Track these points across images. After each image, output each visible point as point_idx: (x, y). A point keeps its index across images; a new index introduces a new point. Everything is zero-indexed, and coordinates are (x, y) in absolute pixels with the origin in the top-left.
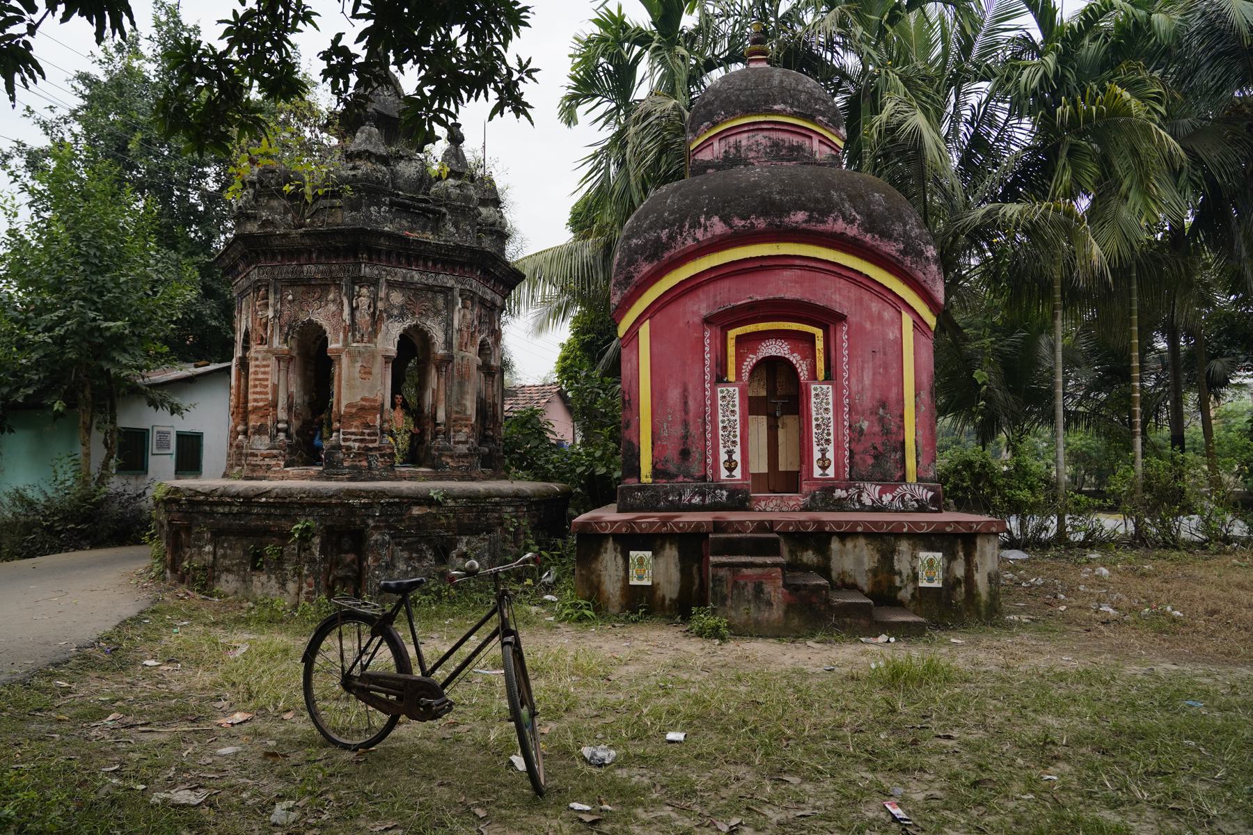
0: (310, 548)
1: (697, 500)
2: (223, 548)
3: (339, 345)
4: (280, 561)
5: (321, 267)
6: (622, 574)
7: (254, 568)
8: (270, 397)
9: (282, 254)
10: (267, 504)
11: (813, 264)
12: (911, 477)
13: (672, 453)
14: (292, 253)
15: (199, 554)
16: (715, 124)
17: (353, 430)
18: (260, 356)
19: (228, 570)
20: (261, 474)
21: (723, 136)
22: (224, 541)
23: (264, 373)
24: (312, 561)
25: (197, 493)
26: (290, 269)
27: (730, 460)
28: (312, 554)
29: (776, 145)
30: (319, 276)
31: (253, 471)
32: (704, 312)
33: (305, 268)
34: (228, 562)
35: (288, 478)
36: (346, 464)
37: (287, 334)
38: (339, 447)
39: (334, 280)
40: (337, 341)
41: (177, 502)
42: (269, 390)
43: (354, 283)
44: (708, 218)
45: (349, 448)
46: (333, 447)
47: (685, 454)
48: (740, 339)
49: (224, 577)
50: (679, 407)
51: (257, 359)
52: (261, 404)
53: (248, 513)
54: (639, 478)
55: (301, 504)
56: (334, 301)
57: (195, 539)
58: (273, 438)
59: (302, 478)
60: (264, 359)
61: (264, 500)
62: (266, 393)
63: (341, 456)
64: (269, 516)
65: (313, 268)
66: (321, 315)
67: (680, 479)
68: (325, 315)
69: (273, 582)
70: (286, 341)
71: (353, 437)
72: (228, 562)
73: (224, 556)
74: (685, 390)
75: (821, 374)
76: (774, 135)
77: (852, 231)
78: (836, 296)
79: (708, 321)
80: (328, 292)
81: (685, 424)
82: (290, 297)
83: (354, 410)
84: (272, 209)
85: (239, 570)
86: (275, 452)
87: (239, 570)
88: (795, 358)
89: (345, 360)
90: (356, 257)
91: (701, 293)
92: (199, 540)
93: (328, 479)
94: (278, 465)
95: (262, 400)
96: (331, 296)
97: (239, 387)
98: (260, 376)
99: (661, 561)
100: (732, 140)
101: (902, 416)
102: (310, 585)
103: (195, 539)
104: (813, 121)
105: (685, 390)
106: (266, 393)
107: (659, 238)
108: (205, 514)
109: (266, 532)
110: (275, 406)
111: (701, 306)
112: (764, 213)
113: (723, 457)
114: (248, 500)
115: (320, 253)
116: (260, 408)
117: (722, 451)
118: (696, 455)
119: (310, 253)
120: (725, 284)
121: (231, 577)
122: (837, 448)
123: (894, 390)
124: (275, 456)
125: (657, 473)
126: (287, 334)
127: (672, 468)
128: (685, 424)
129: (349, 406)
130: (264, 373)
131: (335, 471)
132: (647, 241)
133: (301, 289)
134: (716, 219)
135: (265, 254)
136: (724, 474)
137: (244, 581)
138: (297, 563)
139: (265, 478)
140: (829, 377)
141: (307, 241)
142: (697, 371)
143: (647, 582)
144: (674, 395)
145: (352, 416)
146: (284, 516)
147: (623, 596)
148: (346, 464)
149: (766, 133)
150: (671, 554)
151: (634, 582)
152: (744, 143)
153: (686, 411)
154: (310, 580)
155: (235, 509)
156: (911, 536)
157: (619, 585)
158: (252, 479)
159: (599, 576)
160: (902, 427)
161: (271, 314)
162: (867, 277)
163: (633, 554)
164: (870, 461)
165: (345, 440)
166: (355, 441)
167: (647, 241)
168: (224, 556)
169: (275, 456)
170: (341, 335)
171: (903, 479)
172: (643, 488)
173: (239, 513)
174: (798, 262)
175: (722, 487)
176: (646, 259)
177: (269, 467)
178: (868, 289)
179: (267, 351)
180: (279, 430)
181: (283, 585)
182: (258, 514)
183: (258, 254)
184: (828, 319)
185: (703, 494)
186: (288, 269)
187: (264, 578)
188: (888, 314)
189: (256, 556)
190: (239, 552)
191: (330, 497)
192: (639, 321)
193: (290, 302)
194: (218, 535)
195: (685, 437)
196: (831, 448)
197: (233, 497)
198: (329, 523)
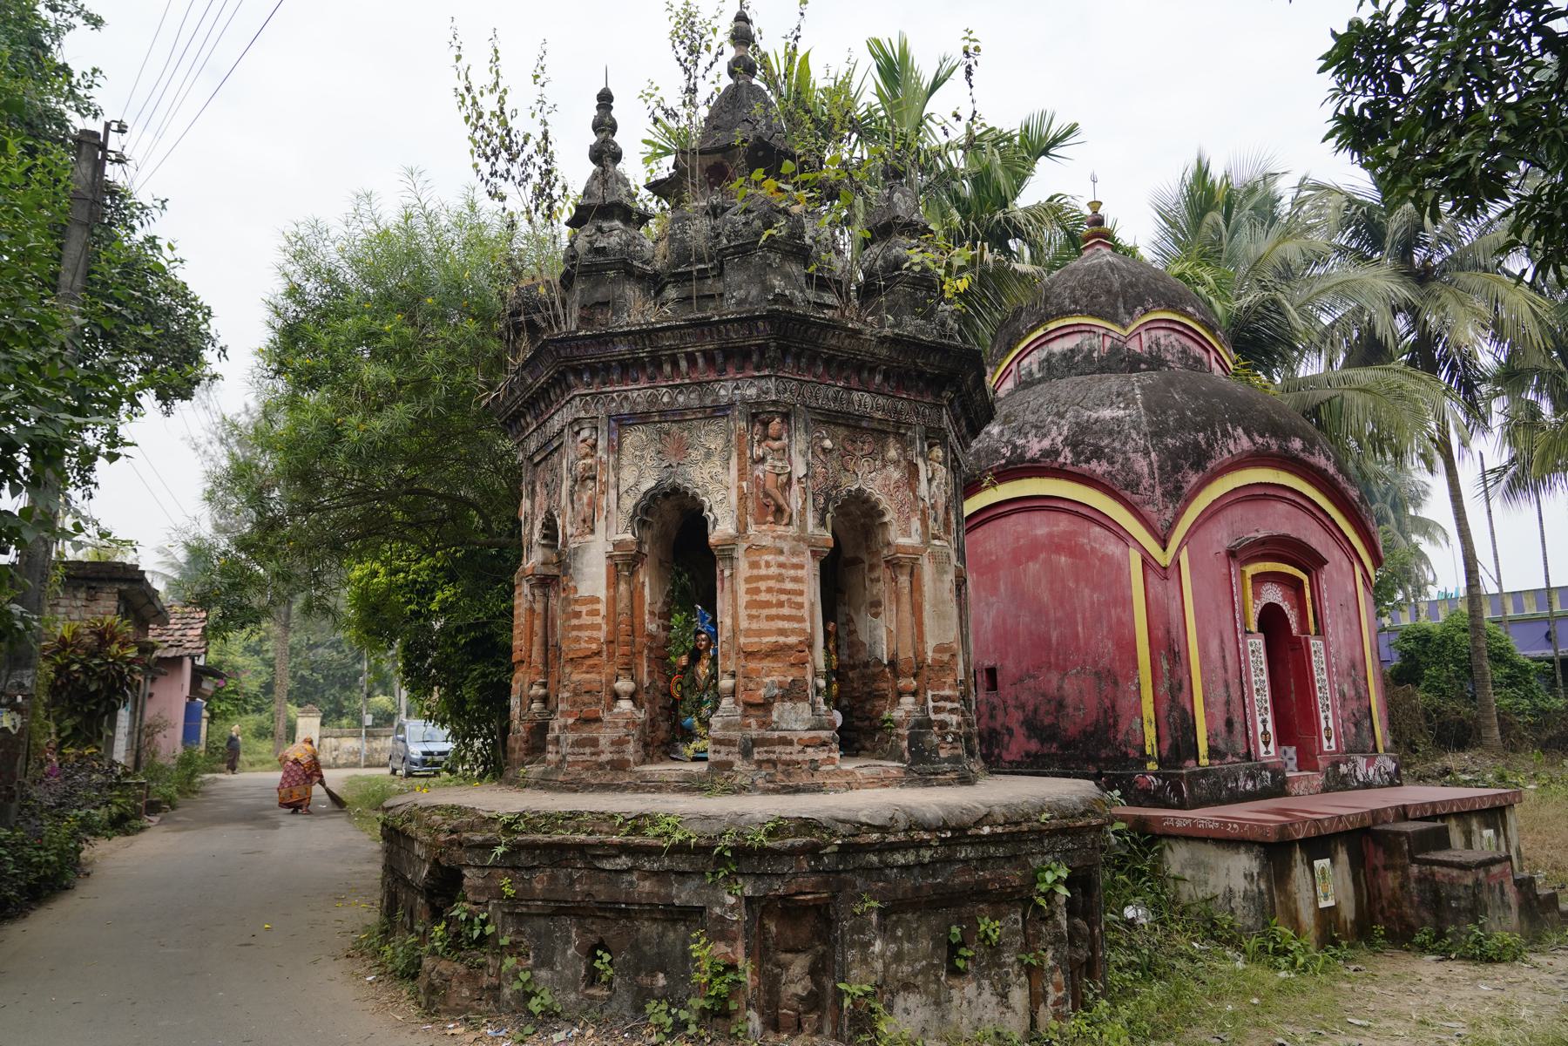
0: (1053, 913)
1: (1249, 786)
2: (895, 939)
3: (914, 540)
4: (996, 950)
5: (881, 401)
6: (1311, 894)
7: (955, 972)
8: (807, 626)
9: (828, 362)
10: (994, 839)
11: (1298, 500)
12: (1381, 750)
13: (1220, 724)
14: (852, 366)
15: (864, 961)
16: (1147, 311)
17: (947, 692)
18: (786, 547)
19: (907, 987)
20: (803, 779)
21: (1149, 327)
22: (896, 925)
23: (795, 580)
24: (1058, 939)
25: (860, 827)
26: (831, 394)
27: (1265, 733)
28: (1057, 925)
29: (1184, 351)
30: (879, 415)
31: (789, 775)
32: (1227, 543)
33: (856, 396)
34: (906, 969)
35: (860, 786)
36: (943, 754)
37: (825, 510)
38: (929, 724)
39: (898, 424)
40: (906, 533)
41: (813, 851)
42: (805, 612)
43: (927, 438)
44: (1234, 429)
45: (943, 725)
46: (919, 724)
47: (1229, 723)
48: (1253, 577)
49: (900, 1002)
50: (1219, 664)
51: (781, 552)
52: (792, 640)
53: (949, 860)
54: (1197, 760)
55: (1040, 832)
56: (896, 463)
57: (853, 930)
58: (813, 705)
59: (883, 782)
60: (794, 553)
61: (986, 830)
62: (801, 619)
63: (936, 740)
64: (983, 861)
65: (867, 398)
66: (876, 480)
67: (1230, 758)
68: (876, 480)
69: (987, 994)
70: (822, 523)
71: (949, 705)
72: (906, 969)
73: (898, 957)
74: (1222, 641)
75: (1312, 628)
76: (1190, 343)
77: (1332, 470)
78: (1315, 538)
79: (1231, 554)
80: (884, 448)
81: (1227, 686)
82: (828, 443)
83: (946, 657)
84: (787, 277)
85: (926, 983)
86: (824, 734)
87: (926, 983)
88: (1286, 607)
89: (927, 569)
90: (938, 395)
91: (1220, 516)
92: (861, 930)
93: (925, 781)
94: (831, 761)
95: (793, 632)
96: (892, 453)
97: (612, 601)
98: (789, 586)
99: (1338, 868)
100: (1153, 333)
101: (1366, 679)
102: (1058, 989)
103: (853, 930)
104: (1214, 336)
105: (1222, 641)
106: (801, 619)
107: (1197, 444)
108: (868, 870)
109: (980, 893)
110: (811, 646)
111: (1222, 536)
112: (1274, 434)
113: (1260, 729)
114: (958, 832)
115: (886, 378)
116: (790, 647)
117: (1259, 719)
118: (1238, 727)
119: (872, 371)
120: (1238, 512)
121: (913, 1000)
122: (1334, 714)
123: (1358, 649)
124: (824, 744)
125: (1213, 752)
126: (825, 510)
127: (1222, 746)
128: (1227, 686)
129: (940, 649)
130: (795, 580)
131: (929, 767)
132: (1186, 444)
133: (842, 432)
134: (1240, 430)
135: (797, 357)
136: (1262, 748)
137: (937, 1004)
138: (1027, 947)
139: (818, 789)
140: (1317, 633)
141: (884, 352)
142: (1229, 615)
143: (1331, 903)
144: (1214, 646)
145: (943, 667)
146: (1008, 859)
147: (1317, 925)
148: (943, 754)
149: (1177, 335)
150: (1343, 857)
151: (1323, 904)
152: (1162, 341)
153: (1226, 671)
154: (1058, 977)
155: (927, 855)
156: (1480, 813)
157: (1311, 910)
158: (797, 790)
159: (1295, 902)
160: (1367, 691)
161: (800, 470)
162: (1333, 521)
163: (1318, 864)
164: (1353, 730)
165: (937, 710)
166: (952, 711)
167: (1186, 444)
168: (898, 957)
169: (824, 744)
170: (916, 523)
171: (1375, 749)
172: (1205, 773)
173: (933, 862)
174: (1289, 495)
175: (1265, 767)
176: (1191, 467)
177: (814, 766)
178: (1332, 534)
179: (799, 539)
180: (818, 691)
181: (1004, 996)
182: (966, 861)
183: (785, 351)
184: (1311, 561)
185: (1252, 777)
186: (827, 393)
187: (970, 989)
188: (1345, 564)
189: (953, 950)
190: (925, 944)
191: (1083, 814)
192: (1180, 548)
193: (824, 450)
194: (893, 910)
195: (1228, 703)
196: (1330, 715)
197: (938, 829)
198: (1077, 864)
